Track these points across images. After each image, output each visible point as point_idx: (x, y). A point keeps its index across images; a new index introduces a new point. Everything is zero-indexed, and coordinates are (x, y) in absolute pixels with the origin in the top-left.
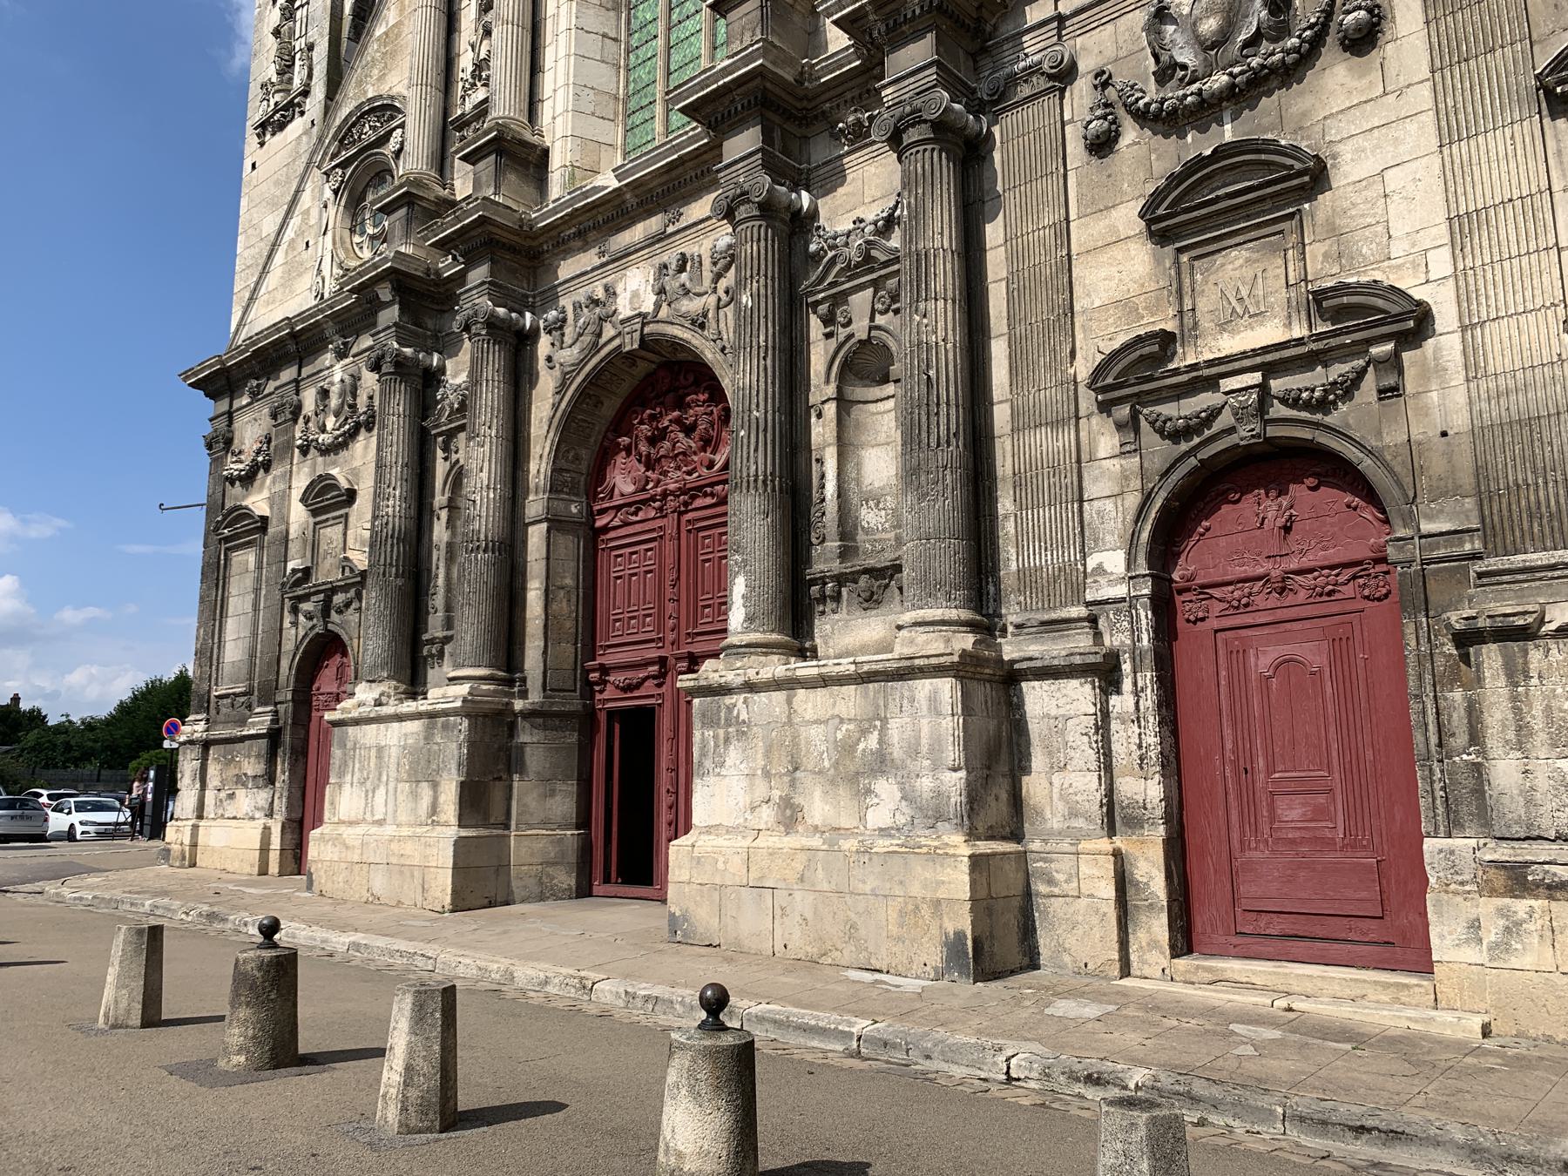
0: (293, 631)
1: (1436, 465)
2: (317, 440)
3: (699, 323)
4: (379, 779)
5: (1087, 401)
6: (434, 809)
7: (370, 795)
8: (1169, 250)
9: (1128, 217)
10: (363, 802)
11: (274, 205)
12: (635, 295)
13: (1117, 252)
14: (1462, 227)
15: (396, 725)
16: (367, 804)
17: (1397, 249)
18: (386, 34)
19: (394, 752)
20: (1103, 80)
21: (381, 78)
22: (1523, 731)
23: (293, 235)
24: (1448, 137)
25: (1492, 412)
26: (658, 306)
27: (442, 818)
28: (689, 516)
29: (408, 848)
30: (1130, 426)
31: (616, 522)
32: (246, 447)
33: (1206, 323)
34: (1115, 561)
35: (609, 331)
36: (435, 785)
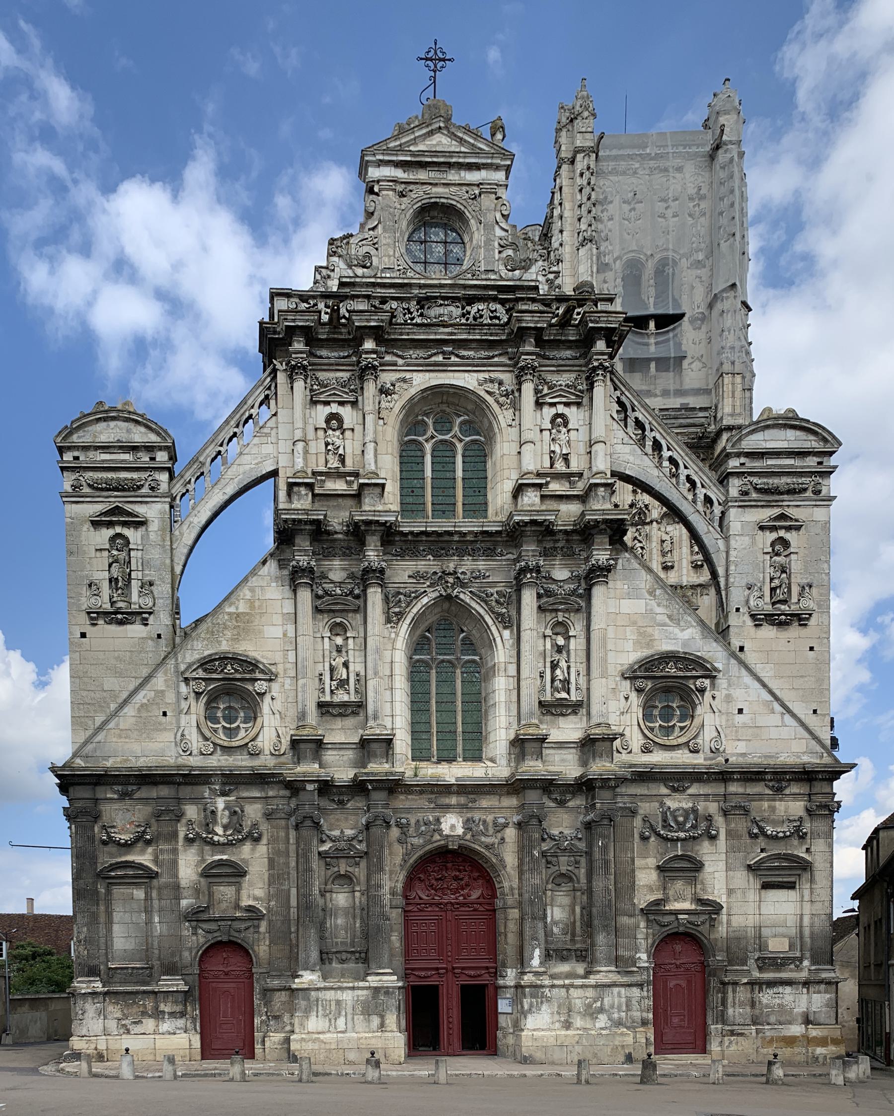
0: (194, 938)
1: (719, 944)
2: (211, 838)
3: (488, 847)
4: (340, 1014)
5: (637, 912)
6: (382, 1025)
7: (333, 1021)
8: (662, 874)
9: (652, 862)
10: (327, 1024)
11: (119, 674)
12: (453, 827)
13: (648, 871)
14: (730, 892)
15: (349, 992)
16: (330, 1025)
17: (716, 892)
18: (238, 615)
19: (350, 1003)
20: (645, 820)
21: (236, 639)
22: (734, 1003)
23: (145, 701)
24: (728, 869)
25: (732, 935)
26: (465, 834)
27: (389, 1029)
28: (456, 913)
29: (373, 1041)
30: (648, 921)
31: (416, 909)
32: (119, 823)
33: (671, 898)
34: (644, 956)
35: (437, 837)
36: (382, 1017)
